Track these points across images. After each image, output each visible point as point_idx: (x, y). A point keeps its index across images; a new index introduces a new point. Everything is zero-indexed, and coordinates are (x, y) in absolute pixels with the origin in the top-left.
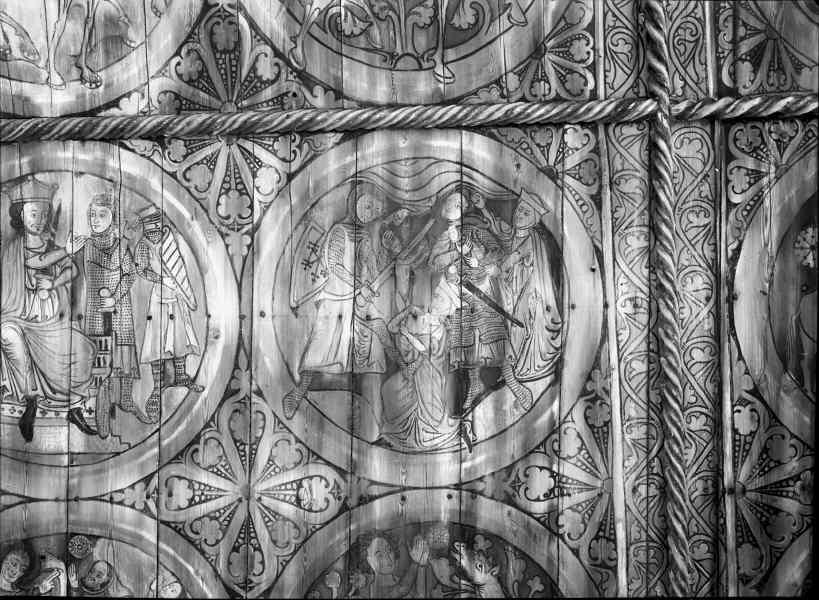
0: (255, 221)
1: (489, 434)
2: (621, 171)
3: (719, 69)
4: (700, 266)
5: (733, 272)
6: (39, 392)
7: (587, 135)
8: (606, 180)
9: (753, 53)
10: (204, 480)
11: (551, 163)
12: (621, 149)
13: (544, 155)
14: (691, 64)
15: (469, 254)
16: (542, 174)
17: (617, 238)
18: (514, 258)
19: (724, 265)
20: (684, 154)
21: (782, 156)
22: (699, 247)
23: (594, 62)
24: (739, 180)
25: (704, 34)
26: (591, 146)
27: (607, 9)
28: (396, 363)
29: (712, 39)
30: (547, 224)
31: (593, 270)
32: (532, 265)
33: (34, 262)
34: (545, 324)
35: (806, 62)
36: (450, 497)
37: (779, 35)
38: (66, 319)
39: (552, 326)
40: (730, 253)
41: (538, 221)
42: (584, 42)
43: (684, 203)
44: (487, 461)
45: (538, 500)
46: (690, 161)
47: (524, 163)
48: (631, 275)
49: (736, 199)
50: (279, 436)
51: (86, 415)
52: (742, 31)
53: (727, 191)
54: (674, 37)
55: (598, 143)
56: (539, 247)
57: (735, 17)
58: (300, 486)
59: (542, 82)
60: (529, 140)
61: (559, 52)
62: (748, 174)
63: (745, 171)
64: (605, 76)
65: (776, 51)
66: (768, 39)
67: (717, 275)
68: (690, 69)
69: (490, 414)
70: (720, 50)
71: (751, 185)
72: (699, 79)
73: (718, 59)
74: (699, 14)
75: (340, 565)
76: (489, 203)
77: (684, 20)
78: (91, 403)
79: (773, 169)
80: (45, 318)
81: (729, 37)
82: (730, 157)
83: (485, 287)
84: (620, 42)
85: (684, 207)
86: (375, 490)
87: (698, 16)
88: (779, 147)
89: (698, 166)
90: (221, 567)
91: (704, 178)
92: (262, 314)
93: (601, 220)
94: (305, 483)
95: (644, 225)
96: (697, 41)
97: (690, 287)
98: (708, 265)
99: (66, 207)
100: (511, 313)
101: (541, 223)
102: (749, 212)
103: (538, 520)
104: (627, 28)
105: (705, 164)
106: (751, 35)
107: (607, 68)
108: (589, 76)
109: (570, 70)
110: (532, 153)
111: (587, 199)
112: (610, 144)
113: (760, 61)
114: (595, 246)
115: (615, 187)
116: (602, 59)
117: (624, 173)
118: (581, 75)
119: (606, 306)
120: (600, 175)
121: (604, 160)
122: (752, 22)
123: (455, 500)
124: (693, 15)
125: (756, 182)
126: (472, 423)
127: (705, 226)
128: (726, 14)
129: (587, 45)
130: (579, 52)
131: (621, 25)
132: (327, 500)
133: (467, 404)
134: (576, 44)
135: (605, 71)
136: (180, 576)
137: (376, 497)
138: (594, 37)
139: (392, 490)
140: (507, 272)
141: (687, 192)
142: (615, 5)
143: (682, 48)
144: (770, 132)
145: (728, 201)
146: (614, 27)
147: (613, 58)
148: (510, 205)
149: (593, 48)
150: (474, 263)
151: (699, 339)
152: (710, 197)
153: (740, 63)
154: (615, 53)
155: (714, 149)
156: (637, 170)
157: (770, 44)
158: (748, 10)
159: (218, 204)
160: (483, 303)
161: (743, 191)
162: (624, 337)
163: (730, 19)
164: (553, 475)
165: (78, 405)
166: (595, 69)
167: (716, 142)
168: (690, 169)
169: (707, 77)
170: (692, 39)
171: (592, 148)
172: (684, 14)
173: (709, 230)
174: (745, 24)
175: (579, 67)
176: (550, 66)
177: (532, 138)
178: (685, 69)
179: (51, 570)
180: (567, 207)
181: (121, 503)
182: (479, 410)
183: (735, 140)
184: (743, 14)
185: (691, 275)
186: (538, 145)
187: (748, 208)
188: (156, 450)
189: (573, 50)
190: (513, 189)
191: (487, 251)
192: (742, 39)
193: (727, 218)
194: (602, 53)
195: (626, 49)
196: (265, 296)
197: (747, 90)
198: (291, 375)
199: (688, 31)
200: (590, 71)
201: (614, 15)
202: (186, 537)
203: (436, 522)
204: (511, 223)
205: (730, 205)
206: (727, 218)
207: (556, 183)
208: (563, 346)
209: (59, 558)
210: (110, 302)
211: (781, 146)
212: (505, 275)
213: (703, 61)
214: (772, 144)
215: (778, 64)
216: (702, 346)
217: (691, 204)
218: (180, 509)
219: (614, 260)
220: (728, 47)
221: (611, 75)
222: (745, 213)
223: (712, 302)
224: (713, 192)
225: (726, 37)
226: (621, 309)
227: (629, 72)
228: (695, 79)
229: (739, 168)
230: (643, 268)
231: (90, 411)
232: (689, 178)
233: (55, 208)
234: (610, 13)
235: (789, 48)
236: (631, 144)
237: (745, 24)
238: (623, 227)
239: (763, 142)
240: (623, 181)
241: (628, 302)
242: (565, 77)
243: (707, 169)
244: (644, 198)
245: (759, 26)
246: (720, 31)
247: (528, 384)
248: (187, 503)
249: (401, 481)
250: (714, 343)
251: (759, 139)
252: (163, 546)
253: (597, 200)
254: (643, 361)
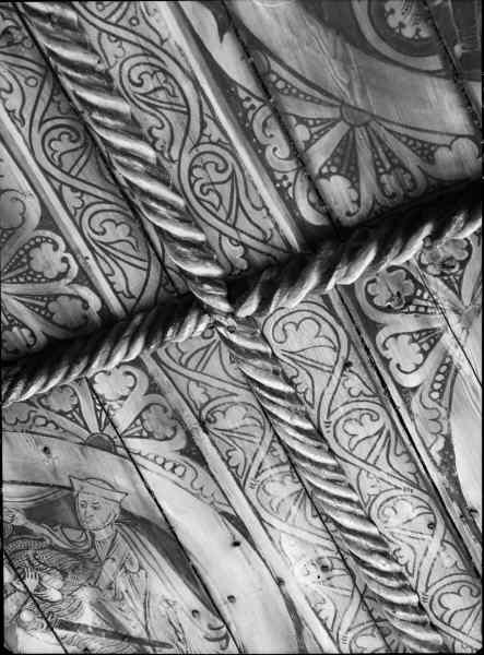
2: (207, 404)
3: (291, 205)
4: (397, 488)
5: (455, 482)
7: (128, 373)
8: (190, 420)
9: (337, 160)
11: (94, 428)
12: (191, 374)
13: (77, 422)
14: (242, 219)
16: (89, 450)
17: (251, 493)
18: (109, 570)
19: (438, 478)
20: (296, 348)
21: (459, 295)
22: (382, 463)
23: (80, 267)
24: (403, 354)
25: (239, 163)
26: (144, 384)
27: (57, 185)
29: (253, 161)
30: (133, 509)
31: (236, 544)
32: (141, 568)
34: (201, 634)
35: (436, 139)
37: (372, 115)
39: (213, 634)
40: (438, 459)
41: (117, 511)
42: (47, 247)
43: (329, 414)
46: (310, 354)
47: (54, 444)
48: (298, 533)
49: (410, 381)
52: (301, 133)
53: (390, 373)
54: (192, 187)
55: (151, 378)
56: (137, 542)
57: (279, 116)
59: (15, 329)
60: (42, 411)
61: (16, 277)
62: (414, 341)
63: (408, 338)
64: (111, 284)
65: (375, 141)
66: (352, 127)
67: (433, 492)
68: (243, 223)
70: (279, 176)
71: (425, 354)
72: (264, 233)
73: (282, 192)
74: (216, 135)
76: (29, 513)
77: (195, 152)
79: (453, 318)
81: (284, 151)
82: (373, 328)
83: (88, 617)
84: (106, 225)
85: (333, 419)
87: (214, 139)
88: (448, 284)
89: (328, 356)
91: (344, 369)
93: (212, 476)
95: (282, 464)
96: (233, 176)
97: (394, 521)
98: (412, 484)
100: (145, 636)
101: (124, 512)
102: (441, 392)
104: (106, 201)
105: (337, 350)
106: (320, 134)
107: (107, 271)
108: (85, 292)
109: (49, 296)
110: (57, 427)
111: (179, 458)
112: (170, 372)
113: (356, 165)
114: (224, 514)
115: (210, 427)
116: (91, 262)
117: (211, 405)
118: (71, 296)
119: (280, 582)
120: (177, 417)
121: (174, 396)
122: (311, 112)
124: (205, 139)
125: (432, 347)
127: (379, 433)
128: (260, 117)
129: (56, 248)
130: (49, 265)
131: (93, 199)
134: (35, 253)
135: (106, 276)
138: (57, 231)
140: (110, 588)
141: (327, 398)
142: (68, 174)
143: (213, 197)
144: (423, 267)
145: (399, 387)
146: (85, 207)
147: (108, 253)
148: (64, 505)
149: (69, 249)
150: (54, 595)
151: (445, 581)
152: (368, 392)
153: (323, 182)
154: (107, 244)
155: (341, 324)
156: (232, 394)
157: (361, 136)
158: (296, 96)
160: (98, 638)
161: (418, 367)
162: (328, 611)
163: (272, 122)
166: (88, 278)
167: (340, 312)
168: (317, 365)
169: (276, 225)
170: (224, 177)
171: (145, 388)
172: (189, 143)
173: (388, 435)
174: (301, 121)
175: (63, 286)
176: (14, 302)
177: (48, 408)
178: (234, 227)
180: (157, 478)
183: (370, 298)
184: (291, 106)
185: (391, 503)
186: (61, 413)
187: (437, 386)
189: (37, 265)
190: (56, 482)
191: (64, 574)
192: (309, 144)
193: (410, 412)
194: (86, 252)
195: (122, 232)
197: (354, 217)
199: (211, 168)
200: (82, 284)
201: (74, 189)
204: (80, 527)
205: (405, 392)
206: (410, 412)
207: (116, 453)
211: (455, 286)
212: (109, 595)
213: (258, 204)
214: (437, 286)
215: (389, 159)
216: (453, 588)
217: (342, 410)
219: (261, 520)
220: (290, 166)
221: (118, 279)
222: (435, 395)
223: (440, 527)
224: (368, 383)
225: (278, 152)
226: (303, 581)
227: (145, 265)
228: (259, 235)
229: (396, 336)
230: (310, 518)
232: (321, 378)
234: (65, 188)
235: (395, 128)
236: (204, 361)
237: (301, 121)
238: (252, 474)
239: (418, 285)
240: (218, 415)
241: (312, 569)
242: (46, 308)
243: (343, 353)
244: (263, 428)
245: (327, 113)
246: (264, 148)
250: (469, 578)
251: (410, 282)
253: (193, 453)
254: (372, 635)
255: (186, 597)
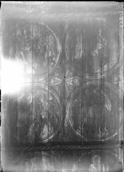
0: (65, 32)
1: (107, 70)
6: (27, 64)
10: (56, 79)
15: (103, 38)
28: (91, 57)
33: (26, 40)
36: (100, 81)
38: (32, 51)
44: (106, 75)
45: (115, 82)
50: (69, 71)
51: (35, 68)
58: (73, 80)
69: (107, 66)
75: (81, 93)
78: (36, 65)
80: (28, 50)
86: (87, 80)
90: (60, 95)
92: (66, 49)
94: (74, 79)
99: (31, 30)
103: (116, 85)
123: (101, 82)
126: (104, 68)
132: (78, 82)
133: (103, 65)
136: (53, 96)
137: (87, 82)
139: (89, 80)
159: (58, 30)
164: (118, 77)
165: (34, 66)
179: (29, 95)
181: (42, 83)
182: (105, 66)
188: (48, 74)
196: (67, 47)
198: (71, 60)
202: (53, 89)
203: (97, 86)
208: (119, 55)
209: (31, 93)
210: (39, 48)
218: (52, 84)
231: (36, 67)
233: (29, 32)
247: (114, 61)
248: (53, 83)
249: (91, 79)
252: (49, 90)
255: (117, 45)
